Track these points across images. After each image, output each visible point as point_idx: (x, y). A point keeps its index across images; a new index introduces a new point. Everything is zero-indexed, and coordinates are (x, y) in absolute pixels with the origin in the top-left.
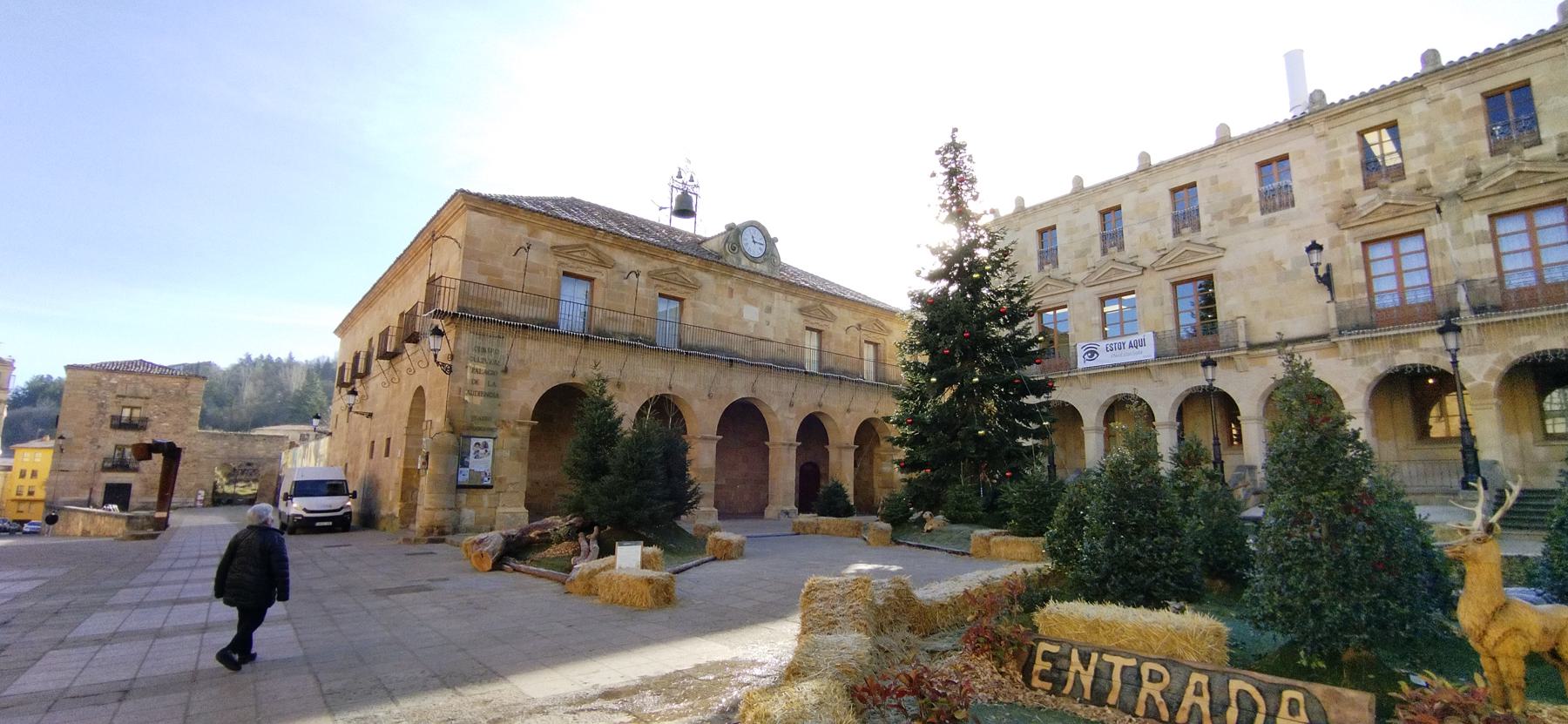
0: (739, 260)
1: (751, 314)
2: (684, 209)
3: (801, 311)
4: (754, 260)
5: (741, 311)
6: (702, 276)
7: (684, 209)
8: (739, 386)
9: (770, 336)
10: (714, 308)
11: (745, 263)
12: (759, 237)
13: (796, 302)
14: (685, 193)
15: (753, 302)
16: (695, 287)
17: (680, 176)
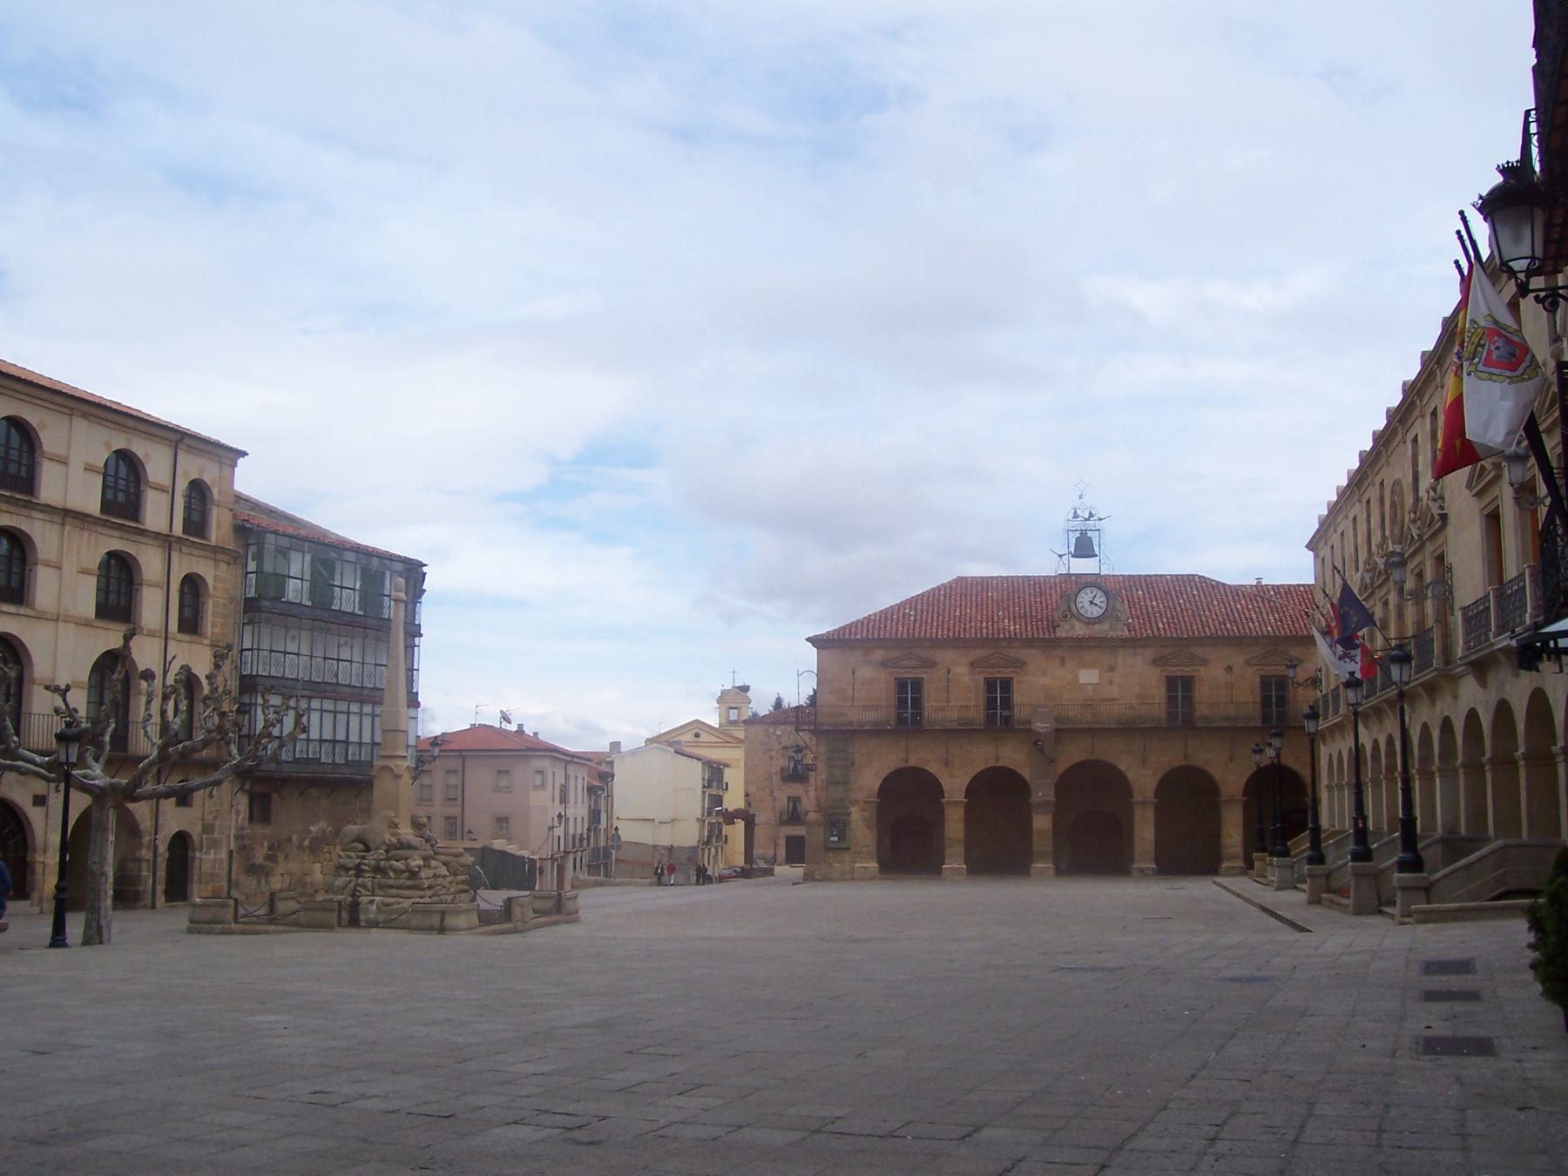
0: (1073, 627)
1: (1089, 676)
2: (1084, 548)
3: (1155, 662)
4: (1091, 622)
5: (1076, 678)
6: (1025, 654)
7: (1084, 548)
8: (1074, 753)
9: (1116, 694)
10: (1045, 681)
11: (1080, 630)
12: (1100, 599)
13: (1149, 653)
14: (1083, 533)
15: (1092, 665)
16: (1020, 664)
17: (1076, 516)
